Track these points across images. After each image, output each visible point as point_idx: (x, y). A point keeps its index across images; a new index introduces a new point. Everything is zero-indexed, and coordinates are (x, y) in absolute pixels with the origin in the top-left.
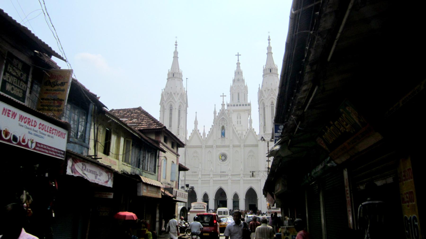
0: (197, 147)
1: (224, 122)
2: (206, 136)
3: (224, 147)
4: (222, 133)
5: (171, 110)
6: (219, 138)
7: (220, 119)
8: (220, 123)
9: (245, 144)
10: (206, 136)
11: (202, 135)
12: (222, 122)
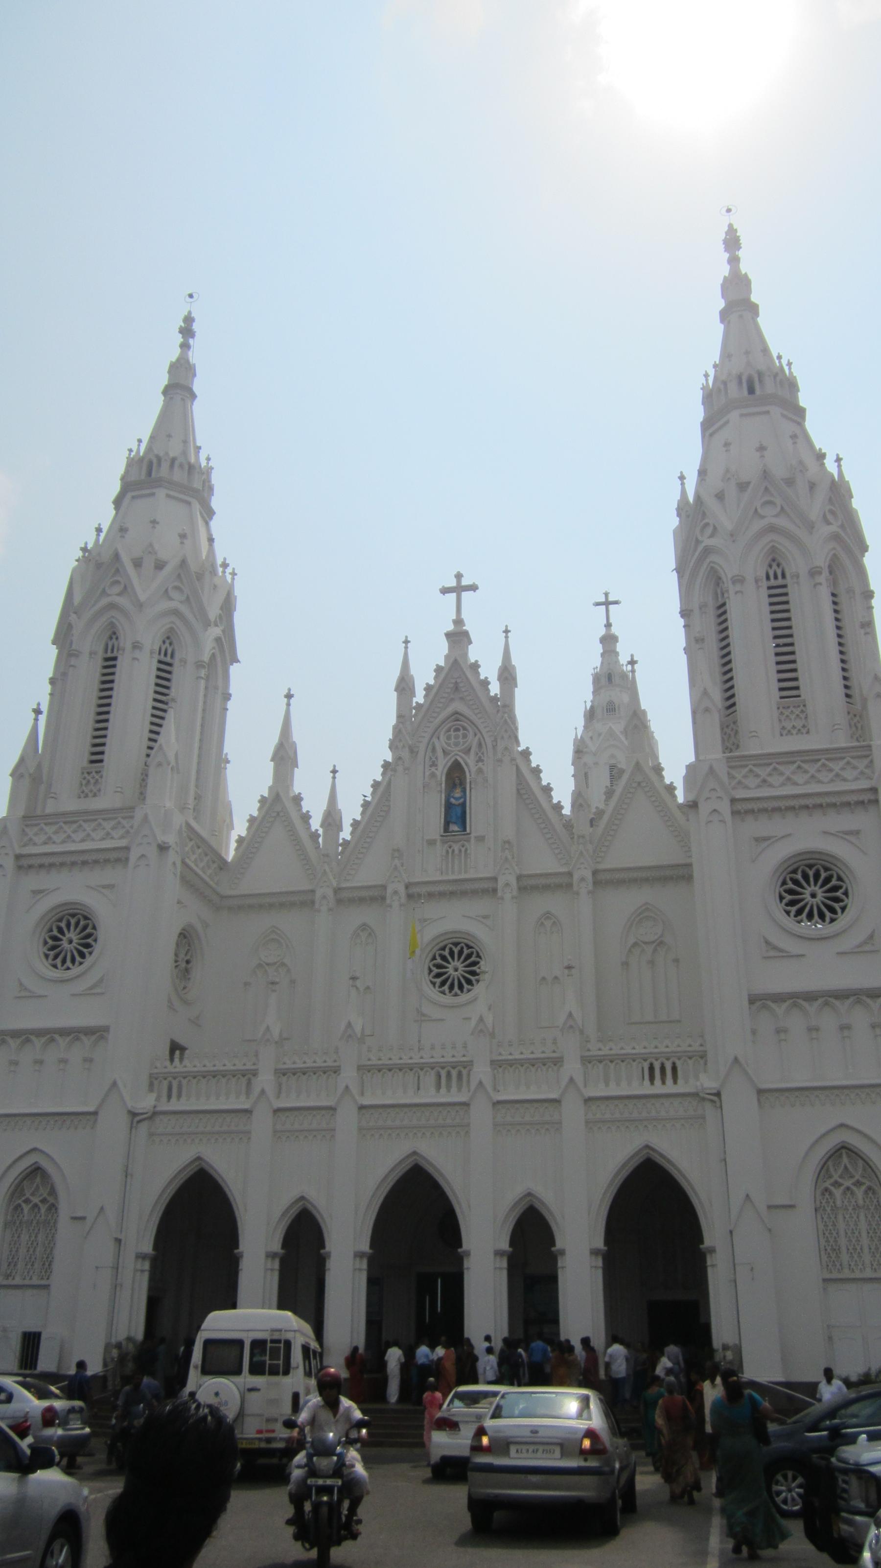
0: (282, 905)
1: (461, 740)
2: (346, 834)
3: (464, 893)
4: (449, 806)
6: (431, 843)
7: (437, 721)
8: (434, 750)
10: (346, 834)
11: (316, 824)
12: (449, 738)
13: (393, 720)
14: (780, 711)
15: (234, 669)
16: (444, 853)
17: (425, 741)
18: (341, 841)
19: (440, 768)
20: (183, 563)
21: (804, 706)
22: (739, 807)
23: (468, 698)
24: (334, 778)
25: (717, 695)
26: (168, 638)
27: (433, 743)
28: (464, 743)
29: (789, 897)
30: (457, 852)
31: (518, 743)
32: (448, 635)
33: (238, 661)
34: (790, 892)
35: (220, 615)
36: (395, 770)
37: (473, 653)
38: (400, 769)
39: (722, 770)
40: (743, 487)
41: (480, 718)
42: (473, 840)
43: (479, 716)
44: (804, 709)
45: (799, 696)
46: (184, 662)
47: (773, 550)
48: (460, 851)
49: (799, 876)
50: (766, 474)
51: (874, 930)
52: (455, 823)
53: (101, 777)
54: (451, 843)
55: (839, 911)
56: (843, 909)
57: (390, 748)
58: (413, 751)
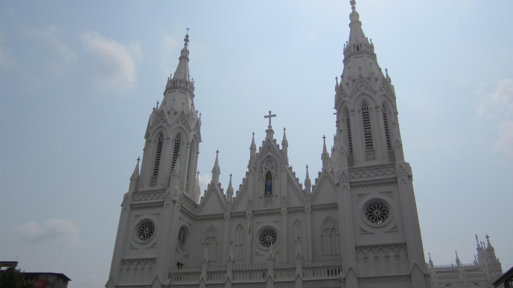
0: (214, 218)
1: (270, 164)
2: (234, 195)
4: (266, 186)
5: (160, 144)
6: (261, 198)
8: (262, 167)
9: (313, 204)
10: (234, 195)
11: (225, 192)
12: (267, 164)
13: (249, 159)
15: (200, 144)
16: (265, 201)
17: (259, 165)
18: (233, 197)
19: (264, 173)
20: (183, 112)
23: (272, 151)
24: (231, 178)
26: (178, 135)
27: (262, 166)
28: (271, 165)
30: (269, 200)
31: (288, 165)
32: (266, 131)
33: (201, 142)
34: (370, 212)
35: (195, 128)
36: (249, 175)
37: (275, 137)
38: (251, 174)
39: (347, 173)
41: (276, 157)
42: (274, 196)
43: (276, 156)
46: (183, 143)
48: (270, 200)
49: (372, 207)
52: (268, 191)
53: (157, 180)
54: (267, 198)
55: (385, 218)
56: (387, 217)
57: (248, 167)
58: (255, 168)
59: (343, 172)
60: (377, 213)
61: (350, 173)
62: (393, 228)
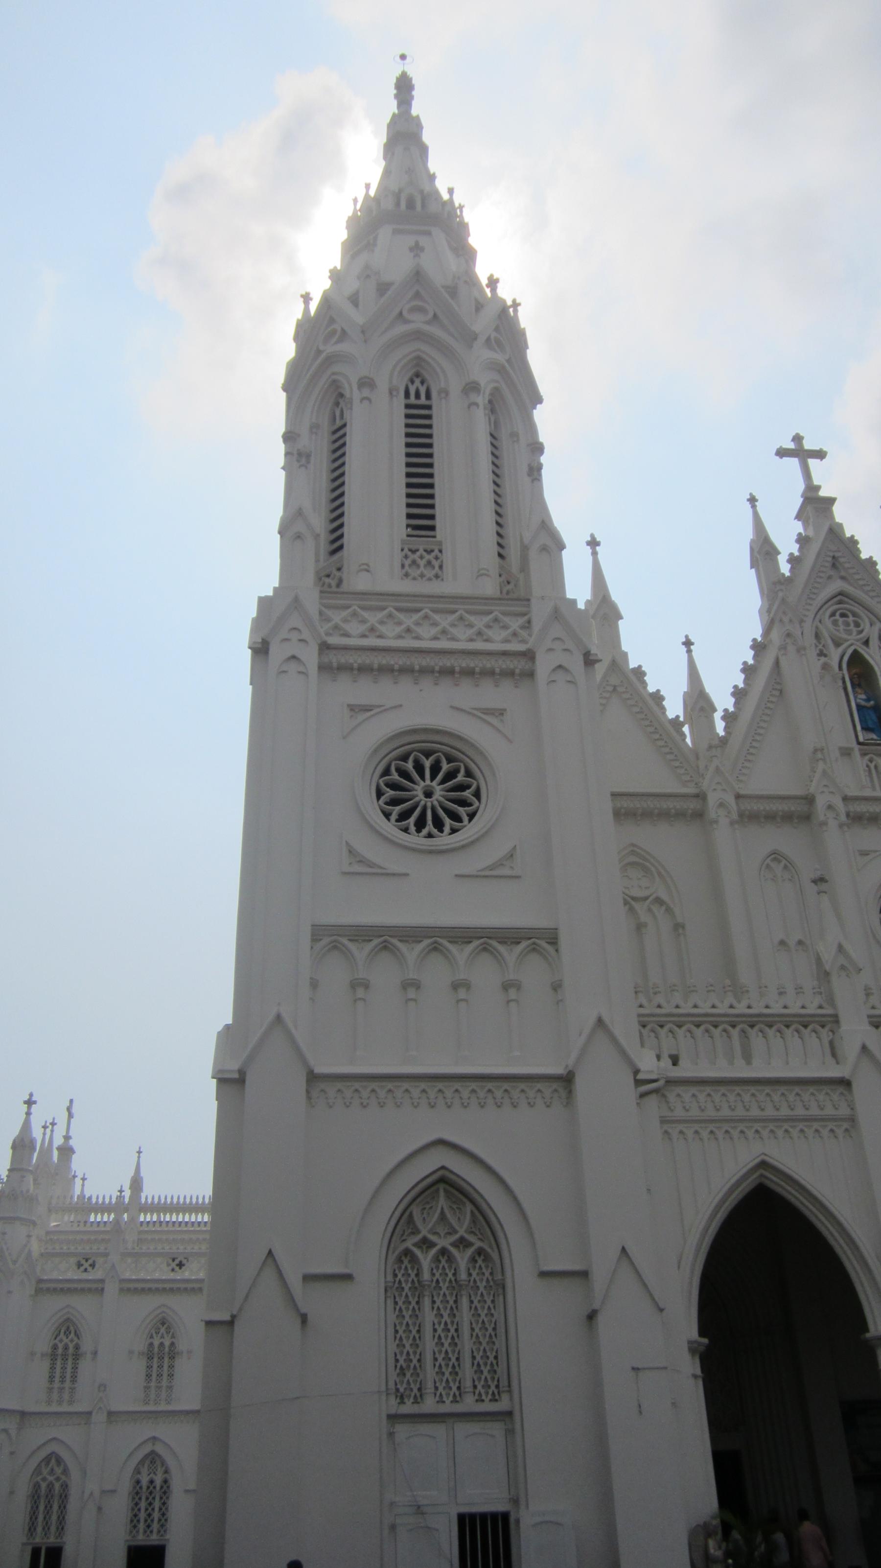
14: (404, 571)
21: (440, 551)
22: (334, 659)
25: (319, 522)
29: (390, 793)
34: (393, 786)
39: (312, 601)
40: (383, 288)
44: (440, 573)
45: (434, 537)
47: (419, 361)
49: (410, 766)
50: (418, 275)
51: (515, 846)
55: (466, 819)
56: (471, 816)
59: (296, 600)
60: (428, 794)
61: (323, 609)
62: (499, 864)
